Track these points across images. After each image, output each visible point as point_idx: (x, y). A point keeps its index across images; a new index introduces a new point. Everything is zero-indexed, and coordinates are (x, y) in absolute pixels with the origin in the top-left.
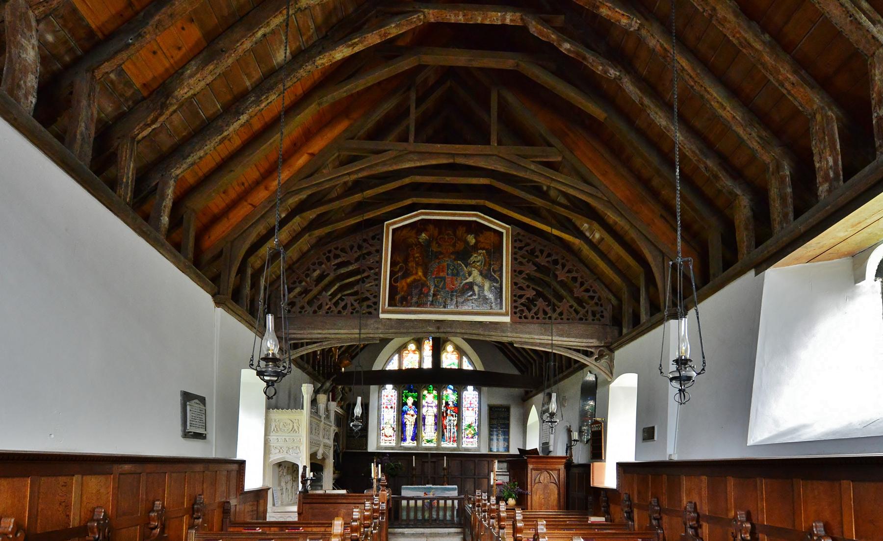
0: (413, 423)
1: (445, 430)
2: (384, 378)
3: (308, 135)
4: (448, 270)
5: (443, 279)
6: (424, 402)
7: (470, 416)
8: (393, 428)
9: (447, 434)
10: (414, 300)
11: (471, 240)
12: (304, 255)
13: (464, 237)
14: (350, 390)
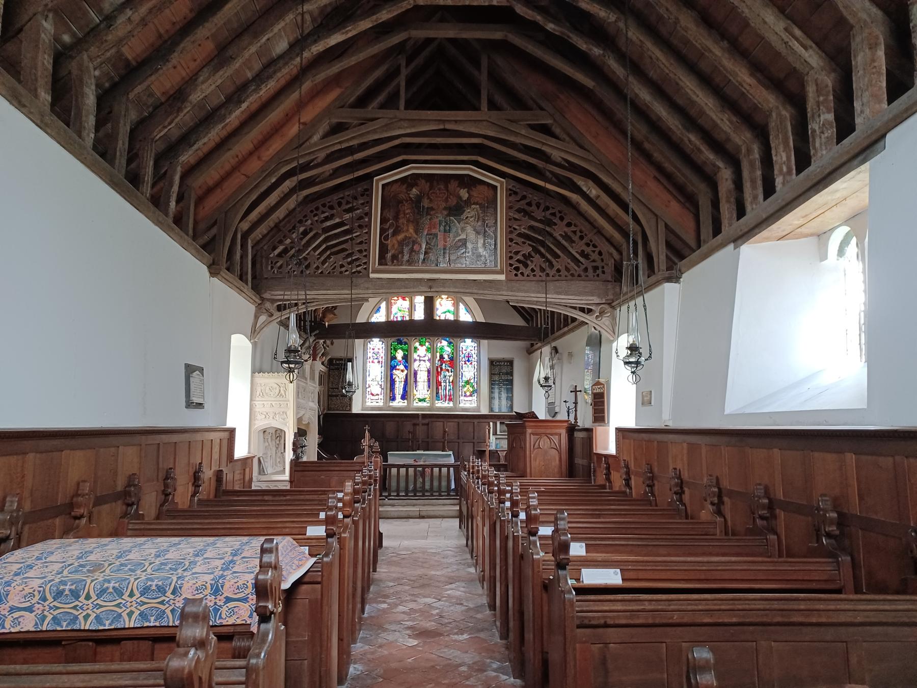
0: (403, 380)
1: (440, 387)
2: (369, 331)
3: (301, 105)
4: (440, 226)
5: (436, 235)
6: (415, 356)
7: (468, 372)
8: (381, 385)
9: (441, 392)
10: (406, 257)
11: (464, 194)
12: (291, 213)
13: (457, 191)
14: (332, 344)
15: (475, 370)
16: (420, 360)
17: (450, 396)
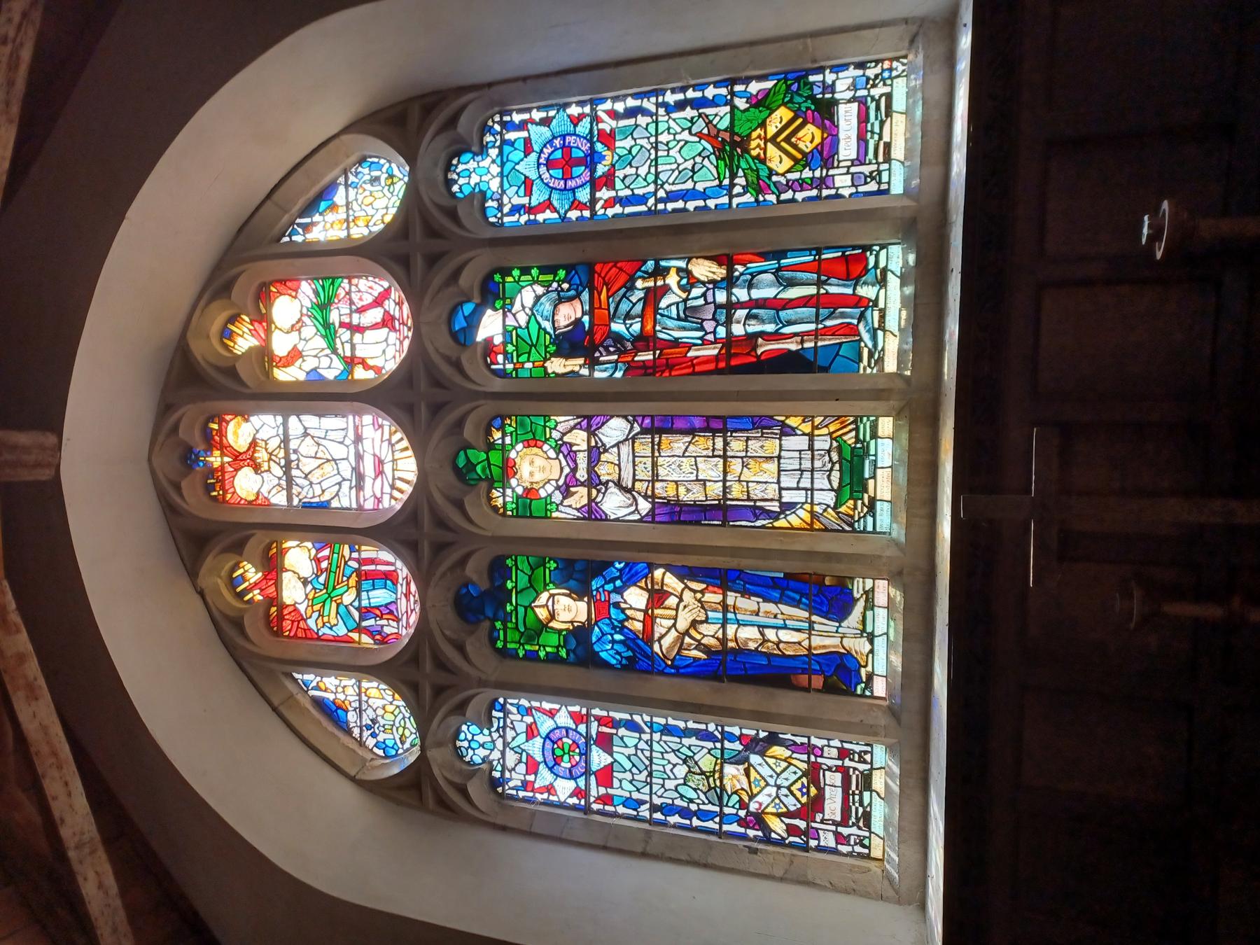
0: (713, 598)
1: (764, 347)
8: (752, 745)
15: (649, 104)
16: (594, 482)
17: (823, 271)
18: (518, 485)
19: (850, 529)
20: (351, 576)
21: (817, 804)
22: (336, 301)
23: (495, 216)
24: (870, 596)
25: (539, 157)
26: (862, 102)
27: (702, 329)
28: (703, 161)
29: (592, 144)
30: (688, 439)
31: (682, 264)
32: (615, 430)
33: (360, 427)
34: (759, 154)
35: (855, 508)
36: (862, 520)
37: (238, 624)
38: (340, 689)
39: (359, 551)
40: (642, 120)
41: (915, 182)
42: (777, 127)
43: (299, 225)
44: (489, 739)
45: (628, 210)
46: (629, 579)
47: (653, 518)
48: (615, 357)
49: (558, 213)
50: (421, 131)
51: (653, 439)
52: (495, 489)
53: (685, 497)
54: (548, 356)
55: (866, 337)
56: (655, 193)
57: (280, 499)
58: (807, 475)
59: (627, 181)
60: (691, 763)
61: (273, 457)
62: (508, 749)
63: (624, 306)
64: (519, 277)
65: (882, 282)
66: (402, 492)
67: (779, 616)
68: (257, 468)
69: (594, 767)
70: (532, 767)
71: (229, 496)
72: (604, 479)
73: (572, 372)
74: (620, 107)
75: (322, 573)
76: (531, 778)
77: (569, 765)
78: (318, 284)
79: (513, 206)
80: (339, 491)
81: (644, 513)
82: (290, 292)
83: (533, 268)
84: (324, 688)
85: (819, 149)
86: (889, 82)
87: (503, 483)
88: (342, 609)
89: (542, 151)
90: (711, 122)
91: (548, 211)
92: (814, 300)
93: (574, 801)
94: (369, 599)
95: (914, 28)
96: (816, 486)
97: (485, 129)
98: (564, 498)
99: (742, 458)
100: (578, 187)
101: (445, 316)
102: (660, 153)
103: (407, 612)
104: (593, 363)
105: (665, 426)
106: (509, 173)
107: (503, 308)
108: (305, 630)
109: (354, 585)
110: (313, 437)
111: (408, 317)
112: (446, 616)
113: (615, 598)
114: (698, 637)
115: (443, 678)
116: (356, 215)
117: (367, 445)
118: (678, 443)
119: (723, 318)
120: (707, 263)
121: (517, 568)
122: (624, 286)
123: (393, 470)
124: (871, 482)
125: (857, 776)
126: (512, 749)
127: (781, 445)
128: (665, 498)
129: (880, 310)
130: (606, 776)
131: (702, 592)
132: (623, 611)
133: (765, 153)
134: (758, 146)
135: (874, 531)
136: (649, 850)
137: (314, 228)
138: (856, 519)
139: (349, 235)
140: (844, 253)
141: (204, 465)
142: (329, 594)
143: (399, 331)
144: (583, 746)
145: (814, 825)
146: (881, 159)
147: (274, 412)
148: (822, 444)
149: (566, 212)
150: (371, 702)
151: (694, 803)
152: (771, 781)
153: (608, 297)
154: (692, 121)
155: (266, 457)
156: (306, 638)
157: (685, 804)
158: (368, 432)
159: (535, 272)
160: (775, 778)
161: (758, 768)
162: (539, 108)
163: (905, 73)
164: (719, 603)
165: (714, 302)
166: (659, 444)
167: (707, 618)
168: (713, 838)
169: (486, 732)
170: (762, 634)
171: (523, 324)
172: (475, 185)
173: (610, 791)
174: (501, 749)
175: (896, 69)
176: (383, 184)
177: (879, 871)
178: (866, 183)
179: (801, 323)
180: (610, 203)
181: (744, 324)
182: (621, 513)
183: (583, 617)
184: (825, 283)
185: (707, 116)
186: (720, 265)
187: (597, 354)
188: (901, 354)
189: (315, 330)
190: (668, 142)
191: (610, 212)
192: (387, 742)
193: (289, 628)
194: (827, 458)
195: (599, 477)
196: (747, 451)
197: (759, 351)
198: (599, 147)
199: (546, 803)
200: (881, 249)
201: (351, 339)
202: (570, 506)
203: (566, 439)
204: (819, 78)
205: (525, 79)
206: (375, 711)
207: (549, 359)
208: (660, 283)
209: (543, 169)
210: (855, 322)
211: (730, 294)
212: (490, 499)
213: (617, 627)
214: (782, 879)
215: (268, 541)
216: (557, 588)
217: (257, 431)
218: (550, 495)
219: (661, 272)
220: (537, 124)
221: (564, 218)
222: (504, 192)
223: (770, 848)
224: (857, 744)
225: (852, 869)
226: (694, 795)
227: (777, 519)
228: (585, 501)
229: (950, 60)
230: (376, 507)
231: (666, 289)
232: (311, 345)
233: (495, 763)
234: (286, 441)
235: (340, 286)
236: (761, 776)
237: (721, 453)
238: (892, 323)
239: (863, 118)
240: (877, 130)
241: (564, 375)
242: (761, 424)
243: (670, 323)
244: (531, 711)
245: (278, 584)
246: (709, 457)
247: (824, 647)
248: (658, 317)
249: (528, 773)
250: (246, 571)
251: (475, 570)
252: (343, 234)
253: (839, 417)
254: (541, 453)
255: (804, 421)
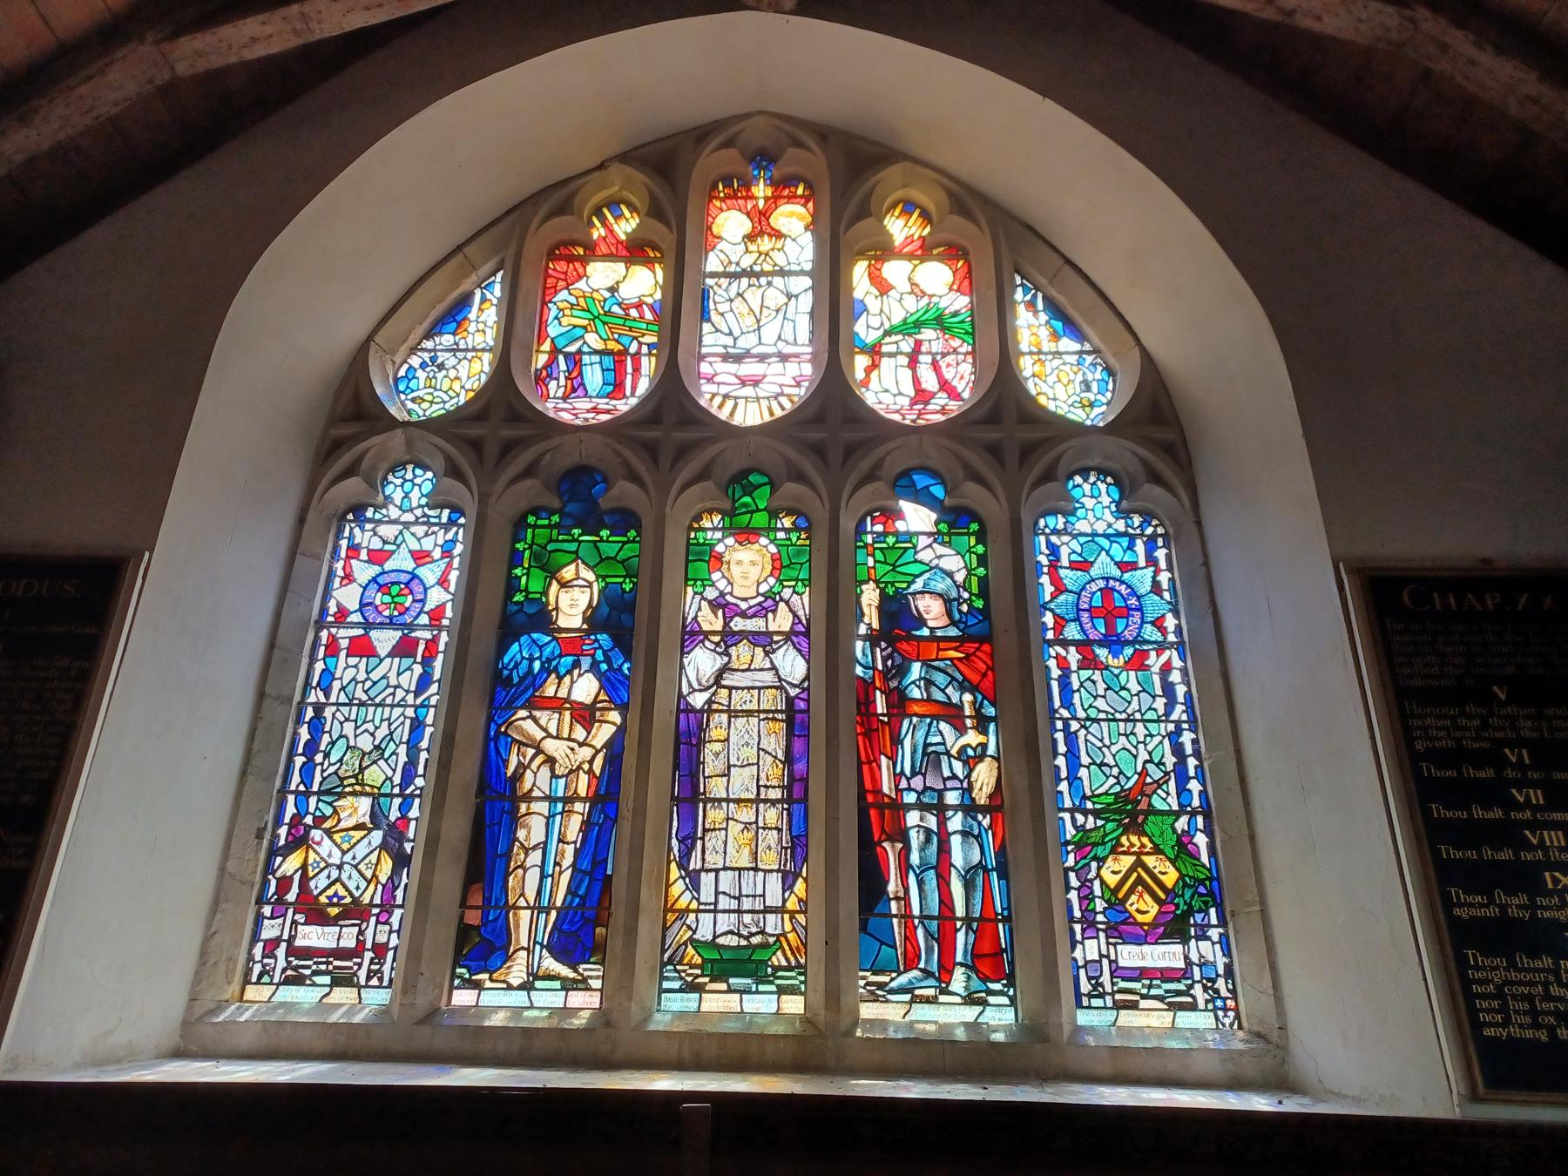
0: (583, 785)
1: (891, 850)
15: (1178, 712)
16: (729, 638)
17: (983, 924)
18: (726, 547)
19: (665, 960)
20: (619, 343)
21: (317, 916)
22: (947, 336)
23: (1046, 526)
24: (580, 986)
25: (1115, 579)
26: (1185, 973)
27: (914, 773)
28: (1114, 776)
29: (1132, 643)
30: (780, 755)
31: (991, 750)
32: (792, 665)
33: (798, 360)
34: (1123, 846)
35: (692, 966)
36: (677, 975)
37: (563, 209)
38: (481, 326)
39: (650, 354)
40: (1160, 704)
41: (1091, 1041)
42: (1155, 867)
43: (1035, 296)
44: (415, 504)
45: (1055, 685)
46: (608, 680)
47: (683, 711)
48: (880, 667)
49: (1051, 601)
50: (1146, 442)
51: (781, 712)
52: (723, 519)
53: (710, 749)
54: (882, 586)
55: (903, 979)
56: (1075, 718)
57: (713, 263)
58: (734, 905)
59: (1088, 684)
60: (375, 755)
61: (763, 257)
62: (401, 527)
63: (940, 679)
64: (974, 553)
65: (970, 1000)
66: (721, 407)
67: (558, 868)
68: (751, 237)
69: (374, 634)
70: (377, 557)
71: (718, 204)
72: (733, 651)
73: (863, 614)
74: (1175, 677)
75: (624, 310)
76: (364, 555)
77: (378, 602)
78: (965, 315)
79: (1058, 547)
80: (722, 333)
81: (690, 699)
82: (958, 282)
83: (986, 569)
84: (483, 307)
85: (1129, 920)
86: (1210, 1006)
87: (731, 528)
88: (579, 332)
89: (1122, 582)
90: (1159, 787)
91: (1053, 589)
92: (948, 914)
93: (333, 609)
94: (591, 364)
95: (1275, 1036)
96: (720, 916)
97: (1148, 516)
98: (710, 602)
99: (756, 822)
100: (1081, 625)
101: (930, 463)
102: (1122, 724)
103: (574, 409)
104: (873, 639)
105: (796, 727)
106: (1097, 544)
107: (939, 532)
108: (555, 287)
109: (609, 347)
110: (786, 304)
111: (927, 420)
112: (569, 456)
113: (586, 662)
114: (534, 766)
115: (491, 451)
116: (1047, 363)
117: (777, 367)
118: (775, 742)
119: (926, 800)
120: (993, 781)
121: (624, 543)
122: (965, 679)
123: (746, 398)
124: (723, 986)
125: (351, 968)
126: (401, 532)
127: (771, 871)
128: (708, 725)
129: (936, 997)
130: (361, 648)
131: (590, 772)
132: (569, 672)
133: (1124, 853)
134: (1132, 845)
135: (662, 991)
136: (267, 702)
137: (1031, 314)
138: (678, 967)
139: (1023, 354)
140: (1006, 951)
141: (755, 177)
142: (598, 317)
143: (911, 409)
144: (401, 620)
145: (290, 911)
146: (1118, 997)
147: (817, 262)
148: (772, 923)
149: (1052, 610)
150: (465, 363)
151: (324, 760)
152: (348, 858)
153: (951, 659)
154: (1160, 764)
155: (764, 248)
156: (545, 288)
157: (322, 748)
158: (792, 369)
159: (981, 571)
160: (352, 862)
161: (366, 841)
162: (1172, 580)
163: (1221, 1026)
164: (575, 792)
165: (946, 789)
166: (774, 719)
167: (558, 777)
168: (278, 783)
169: (424, 501)
170: (535, 848)
171: (920, 556)
172: (1081, 503)
173: (343, 654)
174: (402, 519)
175: (1226, 1016)
176: (1083, 395)
177: (227, 996)
178: (1089, 978)
179: (919, 897)
180: (1063, 663)
181: (918, 826)
182: (690, 671)
183: (563, 622)
184: (969, 927)
185: (1166, 782)
186: (991, 797)
187: (883, 645)
188: (883, 1024)
189: (912, 311)
190: (1134, 734)
191: (1052, 663)
192: (414, 381)
193: (559, 269)
194: (754, 930)
195: (735, 645)
196: (764, 829)
197: (885, 844)
198: (1129, 651)
199: (331, 574)
200: (1009, 997)
201: (901, 353)
202: (699, 609)
203: (782, 605)
204: (1214, 921)
205: (1206, 564)
206: (454, 367)
207: (878, 587)
208: (969, 722)
209: (1102, 584)
210: (922, 965)
211: (956, 808)
212: (710, 512)
213: (550, 666)
214: (222, 870)
215: (663, 247)
216: (600, 591)
217: (794, 240)
218: (713, 585)
219: (982, 724)
220: (1154, 578)
221: (1044, 607)
222: (1075, 537)
223: (262, 856)
224: (392, 969)
225: (232, 960)
226: (335, 759)
227: (680, 866)
228: (705, 627)
229: (1236, 1084)
230: (702, 376)
231: (961, 730)
232: (895, 306)
233: (384, 511)
234: (783, 273)
235: (964, 341)
236: (355, 844)
237: (762, 796)
238: (921, 1012)
239: (1166, 975)
240: (1153, 992)
241: (859, 604)
242: (797, 846)
243: (920, 734)
244: (447, 557)
245: (610, 257)
246: (758, 780)
247: (517, 926)
248: (928, 720)
249: (370, 551)
250: (627, 220)
251: (623, 492)
252: (1024, 347)
253: (805, 945)
254: (765, 575)
255: (800, 900)
